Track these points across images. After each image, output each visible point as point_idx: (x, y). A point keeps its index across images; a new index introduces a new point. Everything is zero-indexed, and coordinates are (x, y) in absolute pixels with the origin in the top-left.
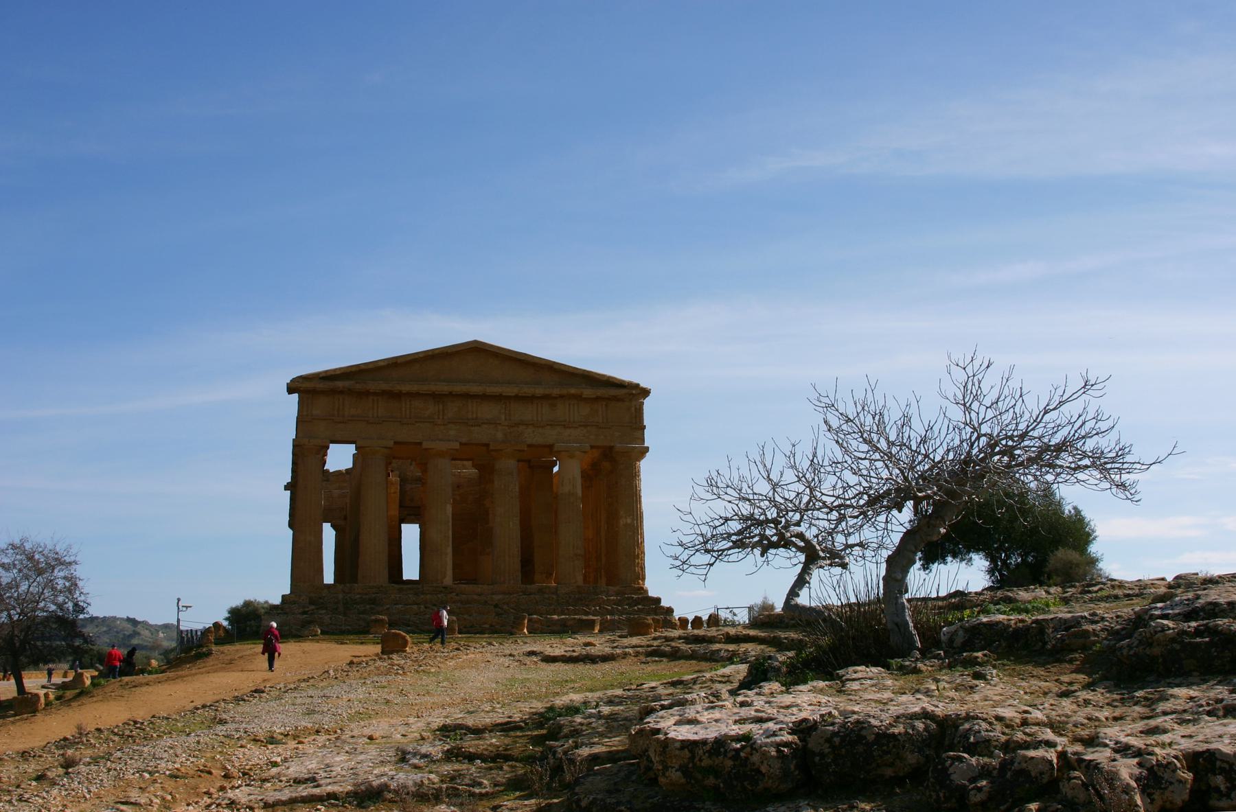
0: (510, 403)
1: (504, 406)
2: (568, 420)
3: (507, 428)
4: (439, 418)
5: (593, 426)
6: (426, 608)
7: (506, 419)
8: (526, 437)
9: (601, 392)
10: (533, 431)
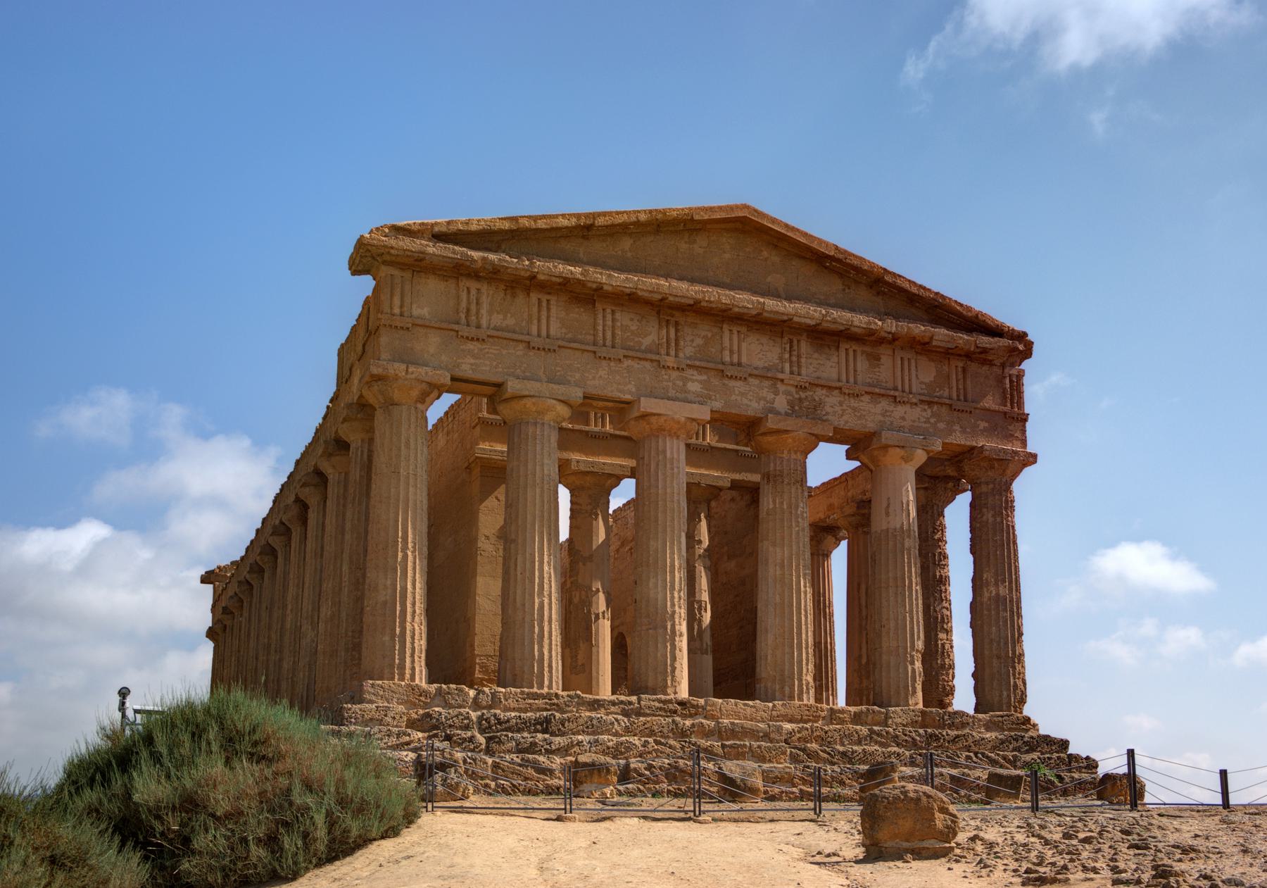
0: (798, 341)
1: (788, 349)
2: (900, 388)
4: (668, 354)
5: (942, 404)
6: (655, 741)
7: (792, 373)
8: (827, 414)
9: (963, 339)
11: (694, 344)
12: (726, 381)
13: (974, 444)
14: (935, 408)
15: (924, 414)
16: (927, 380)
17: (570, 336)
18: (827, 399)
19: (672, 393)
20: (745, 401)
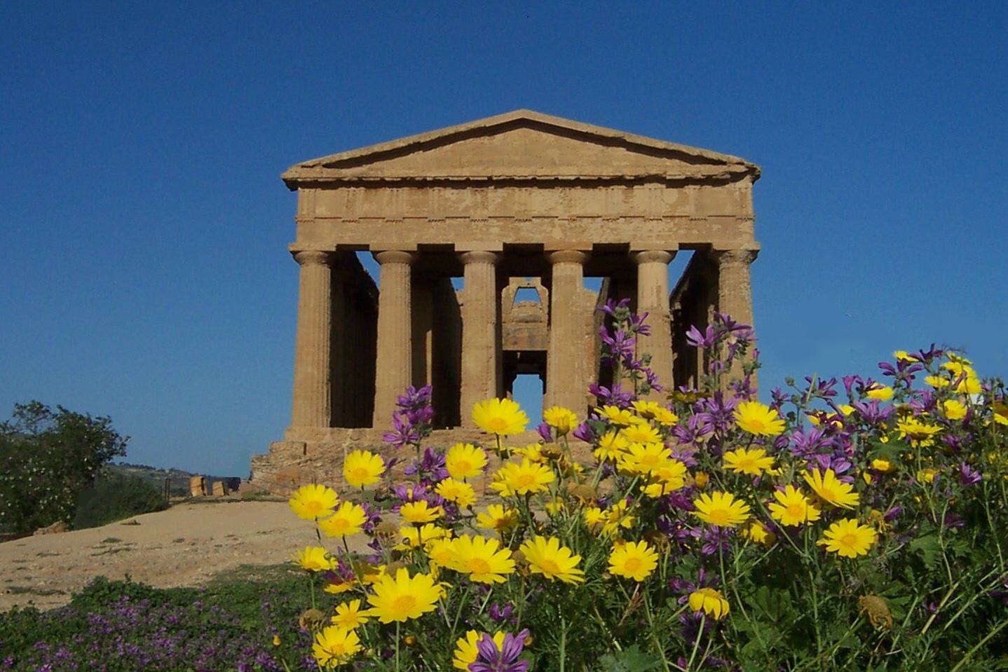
3: (566, 222)
10: (602, 227)
11: (496, 203)
12: (517, 224)
13: (709, 241)
14: (677, 220)
15: (668, 226)
16: (671, 202)
17: (412, 210)
18: (591, 226)
19: (479, 236)
20: (531, 235)
